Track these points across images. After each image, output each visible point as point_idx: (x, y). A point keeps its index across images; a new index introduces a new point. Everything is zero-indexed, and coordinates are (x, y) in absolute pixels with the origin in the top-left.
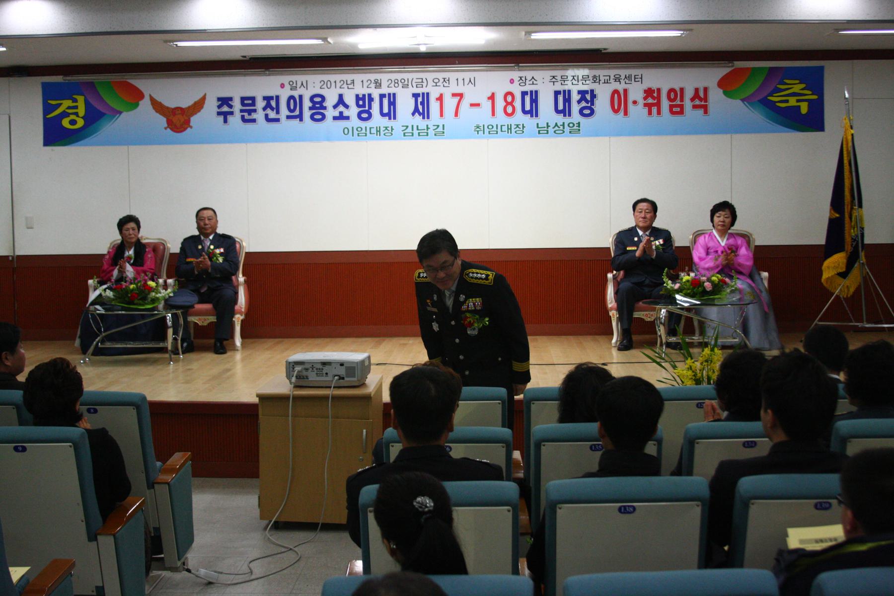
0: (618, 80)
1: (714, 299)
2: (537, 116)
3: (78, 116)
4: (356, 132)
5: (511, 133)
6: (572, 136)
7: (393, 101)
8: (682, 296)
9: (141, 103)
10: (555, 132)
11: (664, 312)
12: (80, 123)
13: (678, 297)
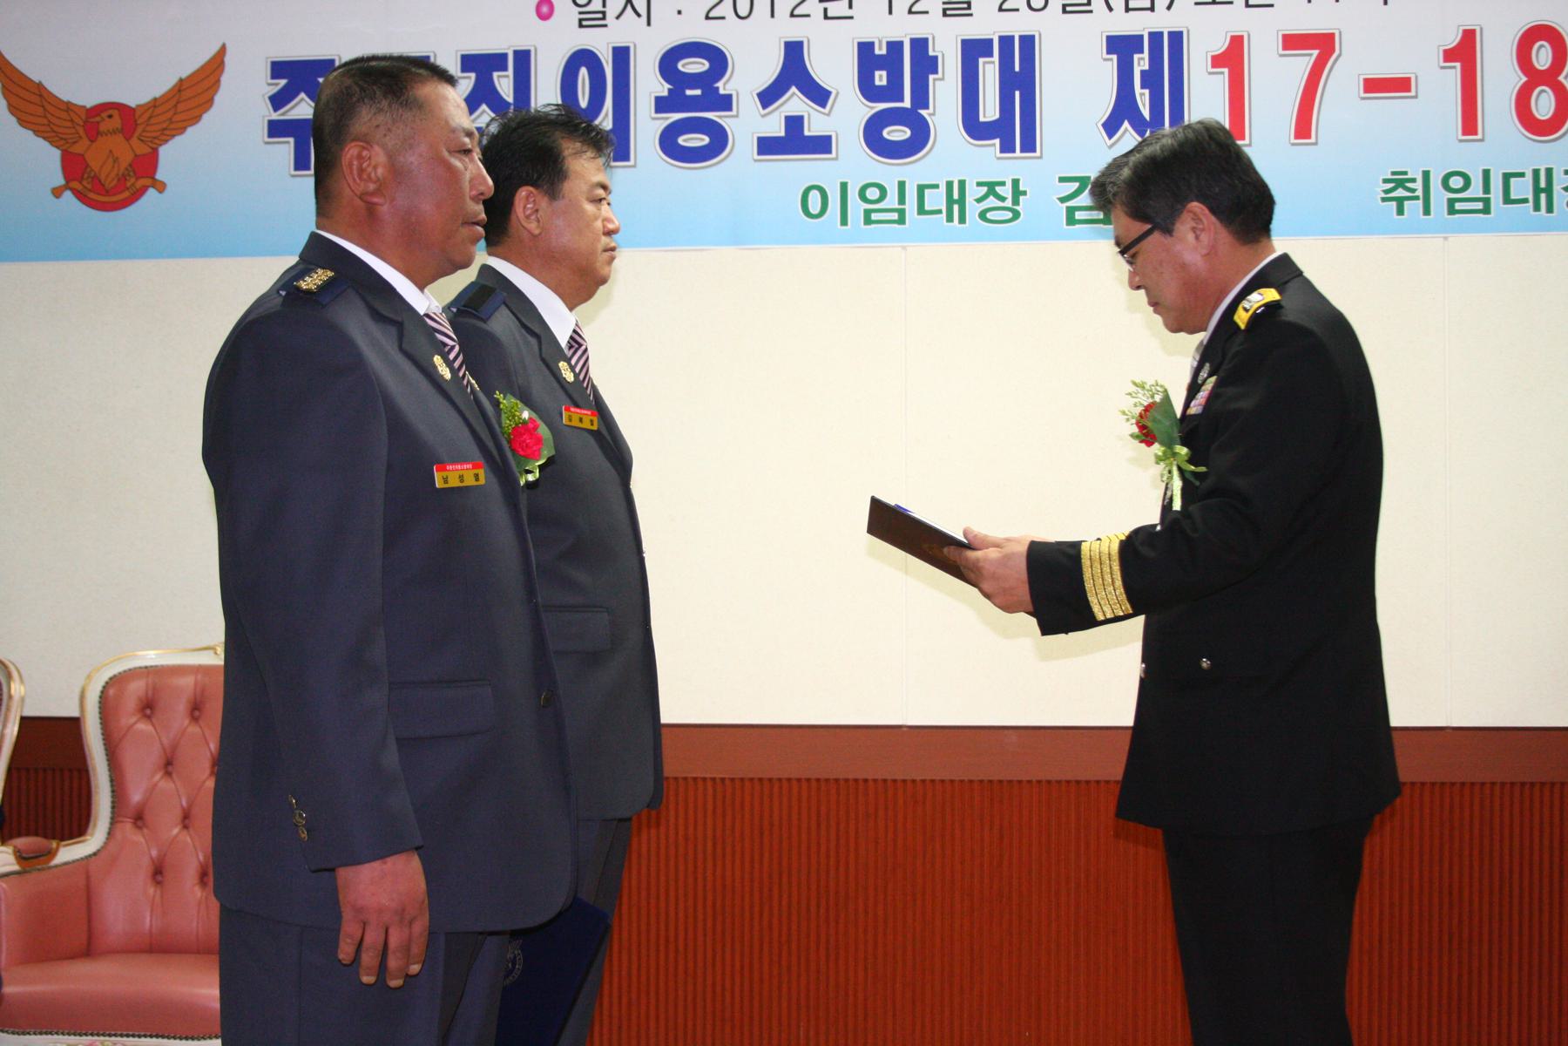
4: (856, 207)
5: (1550, 209)
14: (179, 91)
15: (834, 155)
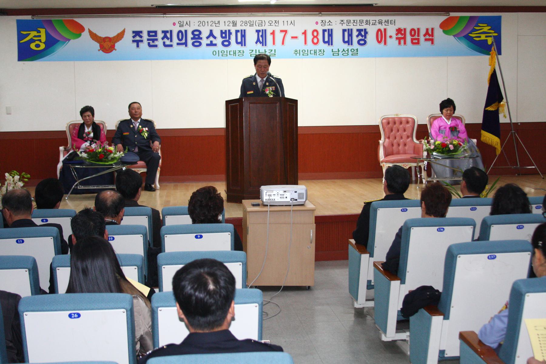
0: (381, 23)
1: (454, 155)
2: (332, 44)
4: (220, 54)
5: (316, 55)
6: (353, 57)
8: (436, 153)
10: (343, 54)
11: (426, 163)
12: (43, 46)
13: (434, 153)
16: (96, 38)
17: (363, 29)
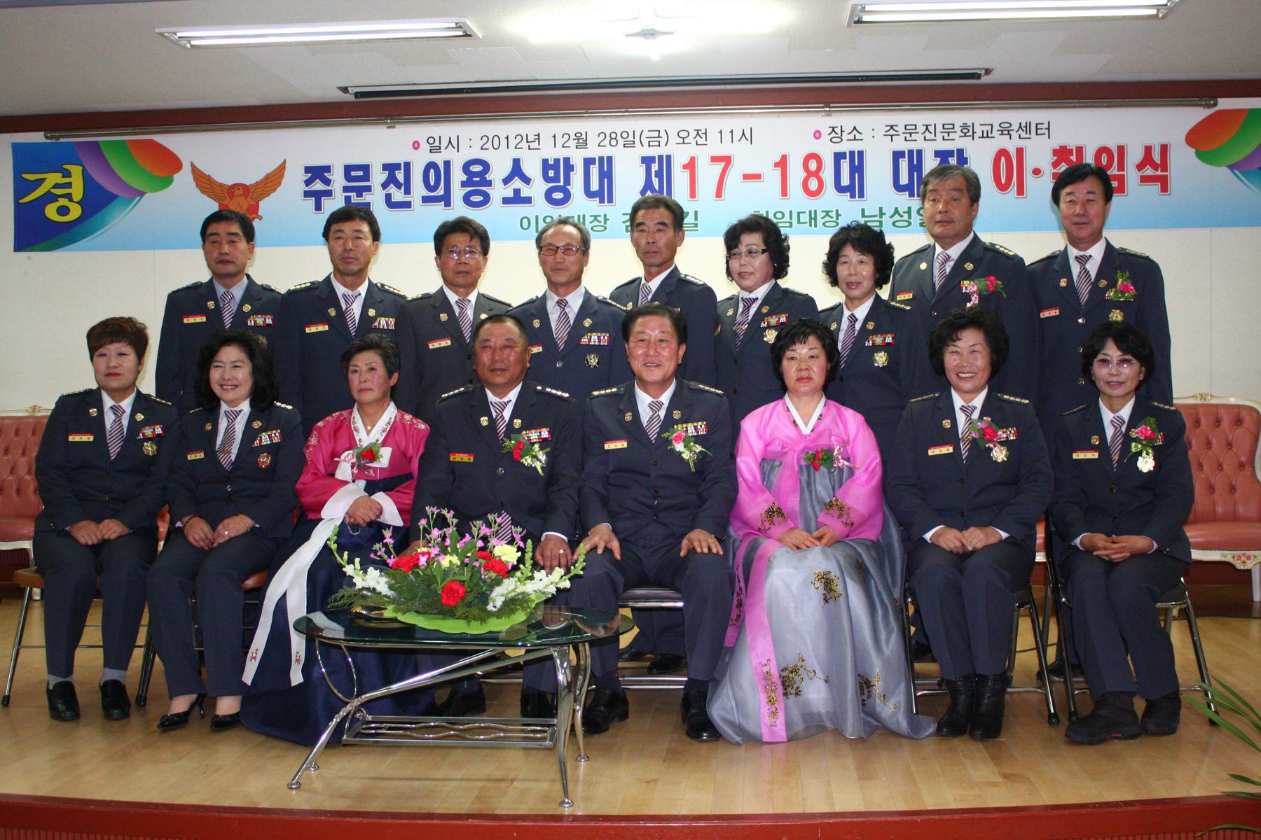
0: (1006, 132)
2: (861, 195)
3: (71, 200)
5: (816, 226)
7: (607, 169)
9: (176, 177)
10: (894, 224)
12: (75, 212)
14: (267, 178)
15: (533, 204)
16: (209, 187)
17: (953, 151)
